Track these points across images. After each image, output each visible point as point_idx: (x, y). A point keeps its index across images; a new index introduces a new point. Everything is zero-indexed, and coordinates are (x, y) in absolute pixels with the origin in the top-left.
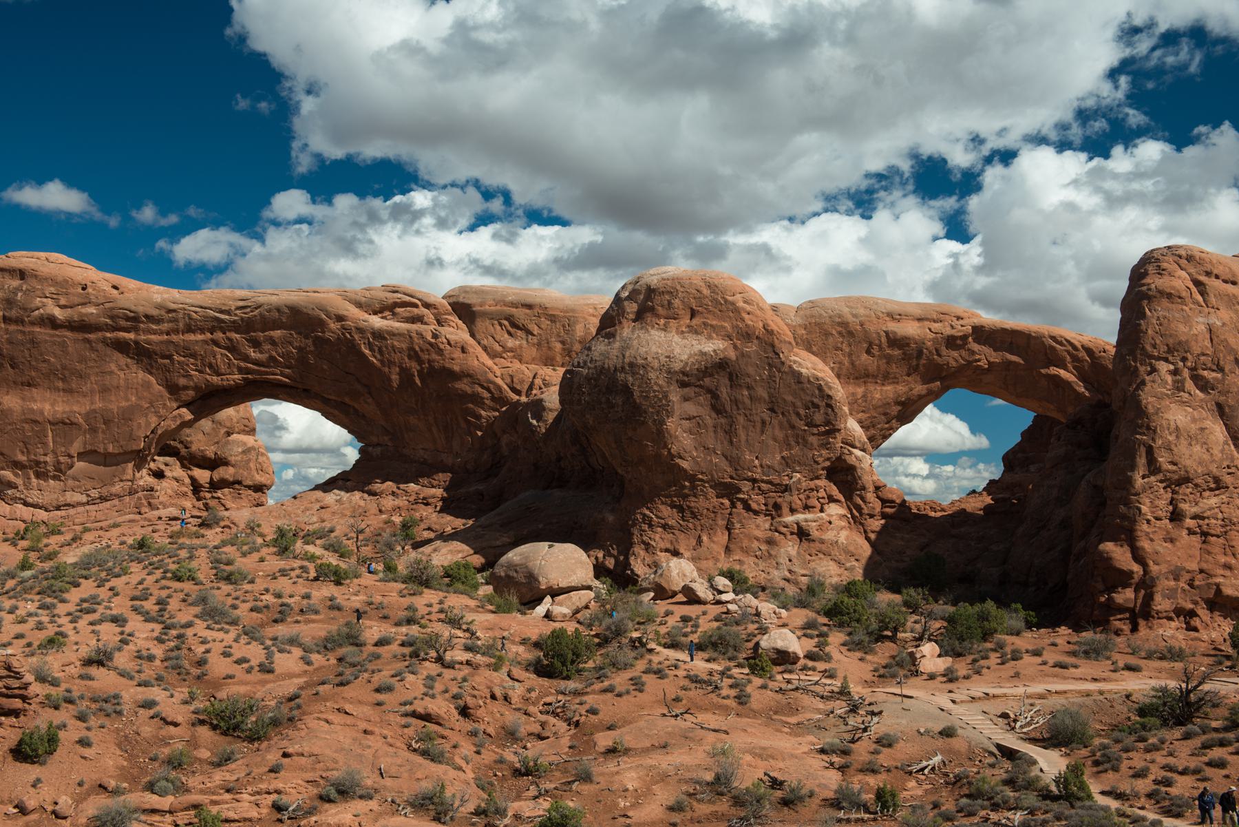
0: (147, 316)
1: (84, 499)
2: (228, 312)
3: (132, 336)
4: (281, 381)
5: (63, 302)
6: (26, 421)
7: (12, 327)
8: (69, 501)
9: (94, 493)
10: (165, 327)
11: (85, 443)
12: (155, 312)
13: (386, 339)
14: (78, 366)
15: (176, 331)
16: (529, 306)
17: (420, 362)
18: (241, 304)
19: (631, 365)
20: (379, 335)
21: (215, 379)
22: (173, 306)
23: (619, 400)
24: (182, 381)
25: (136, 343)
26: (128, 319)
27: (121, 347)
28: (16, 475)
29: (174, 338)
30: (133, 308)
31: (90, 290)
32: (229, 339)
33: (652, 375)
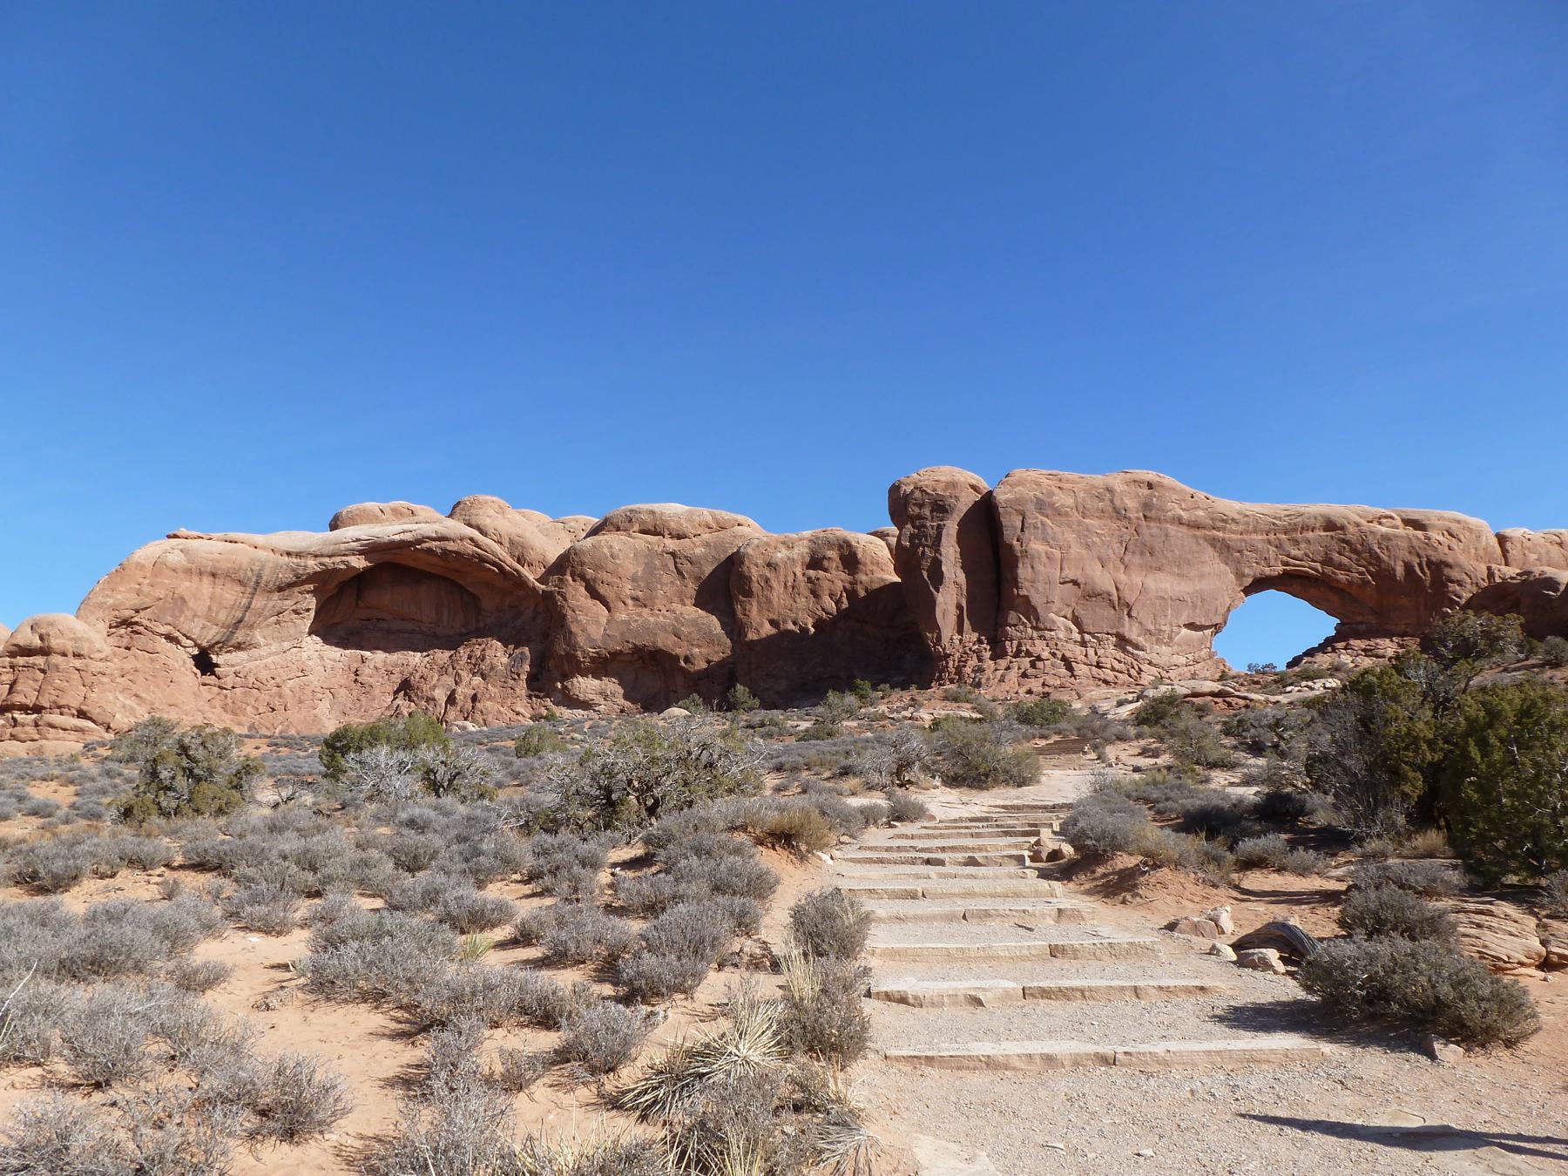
0: (1233, 519)
2: (1280, 519)
5: (1184, 506)
10: (1241, 528)
11: (1188, 616)
12: (1237, 517)
13: (1390, 539)
14: (1190, 557)
15: (1248, 532)
16: (1459, 522)
17: (1419, 556)
21: (1267, 571)
22: (1248, 513)
25: (1223, 539)
26: (1223, 520)
28: (1146, 640)
31: (1195, 498)
32: (1279, 540)
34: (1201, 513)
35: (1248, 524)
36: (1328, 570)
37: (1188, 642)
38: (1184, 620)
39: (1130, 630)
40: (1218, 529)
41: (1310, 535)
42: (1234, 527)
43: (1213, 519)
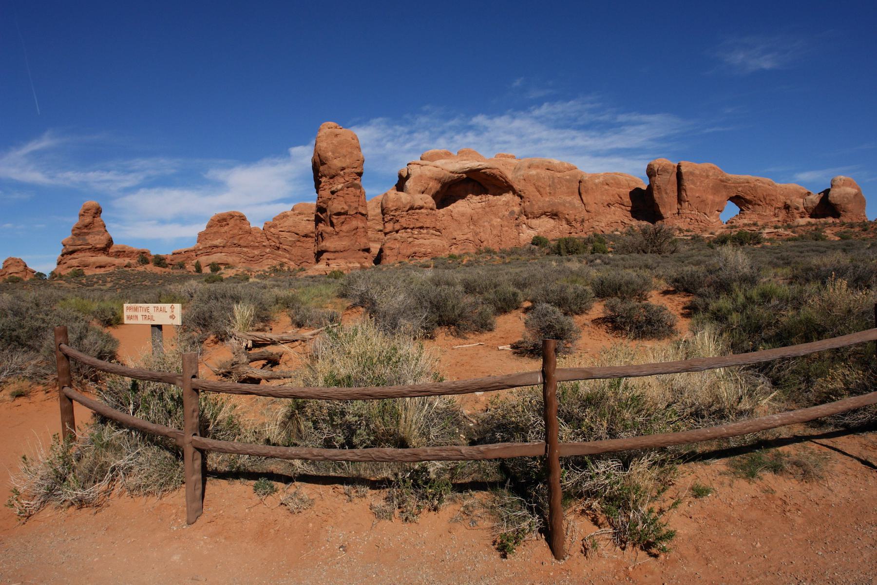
20: (760, 187)
41: (743, 185)
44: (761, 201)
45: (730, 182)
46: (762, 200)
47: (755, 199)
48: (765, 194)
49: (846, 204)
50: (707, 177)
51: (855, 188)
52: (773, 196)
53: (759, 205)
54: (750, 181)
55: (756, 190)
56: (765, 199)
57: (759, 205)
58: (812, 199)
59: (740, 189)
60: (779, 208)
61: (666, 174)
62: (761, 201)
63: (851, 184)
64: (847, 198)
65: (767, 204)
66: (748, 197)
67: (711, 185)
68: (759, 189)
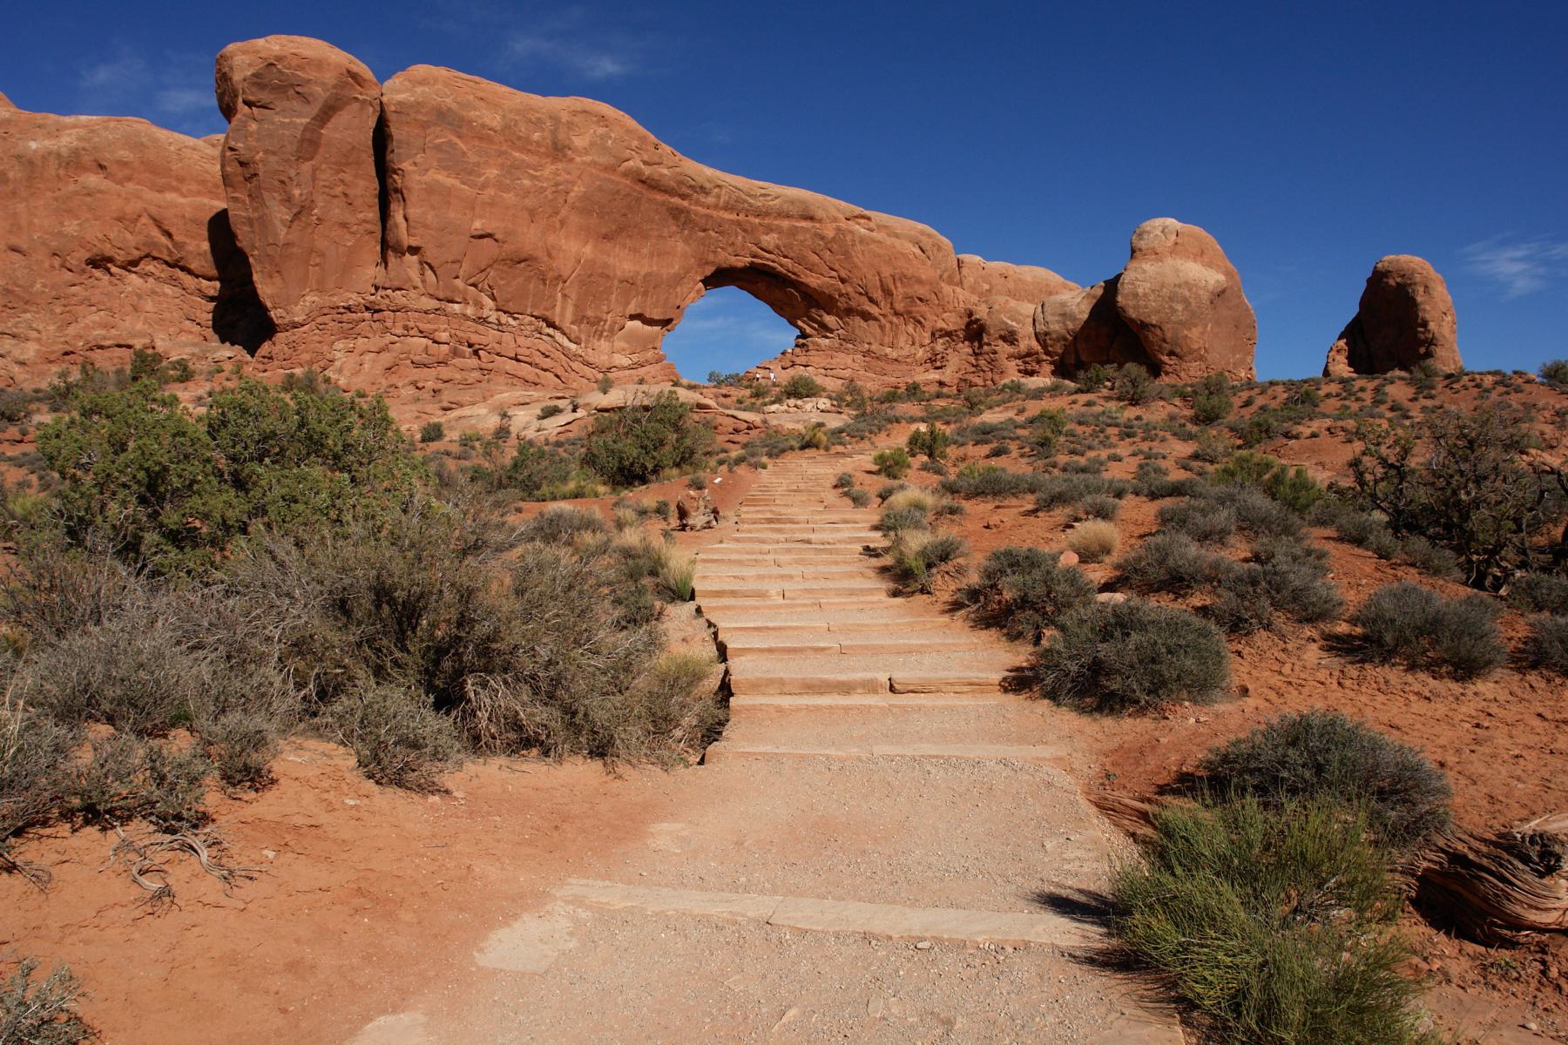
0: (702, 187)
1: (626, 362)
2: (754, 196)
3: (686, 203)
4: (774, 268)
6: (602, 275)
7: (603, 175)
8: (617, 363)
9: (635, 358)
10: (711, 200)
12: (707, 185)
15: (716, 207)
18: (763, 191)
19: (1186, 283)
22: (720, 183)
23: (1179, 307)
24: (711, 257)
25: (688, 212)
26: (691, 187)
27: (676, 213)
29: (714, 213)
30: (696, 178)
33: (1201, 292)
34: (665, 171)
35: (718, 196)
36: (798, 269)
37: (633, 337)
38: (632, 308)
39: (562, 315)
40: (683, 197)
41: (785, 224)
42: (702, 198)
43: (681, 183)
44: (871, 300)
45: (711, 200)
46: (878, 295)
47: (849, 289)
48: (887, 272)
49: (1182, 324)
50: (558, 151)
51: (1218, 268)
52: (920, 281)
53: (866, 316)
54: (820, 214)
55: (846, 253)
56: (887, 293)
57: (866, 316)
58: (1063, 304)
59: (769, 240)
60: (949, 334)
61: (296, 104)
62: (871, 300)
63: (1202, 253)
64: (1185, 301)
65: (896, 314)
66: (813, 280)
67: (578, 190)
68: (859, 247)
